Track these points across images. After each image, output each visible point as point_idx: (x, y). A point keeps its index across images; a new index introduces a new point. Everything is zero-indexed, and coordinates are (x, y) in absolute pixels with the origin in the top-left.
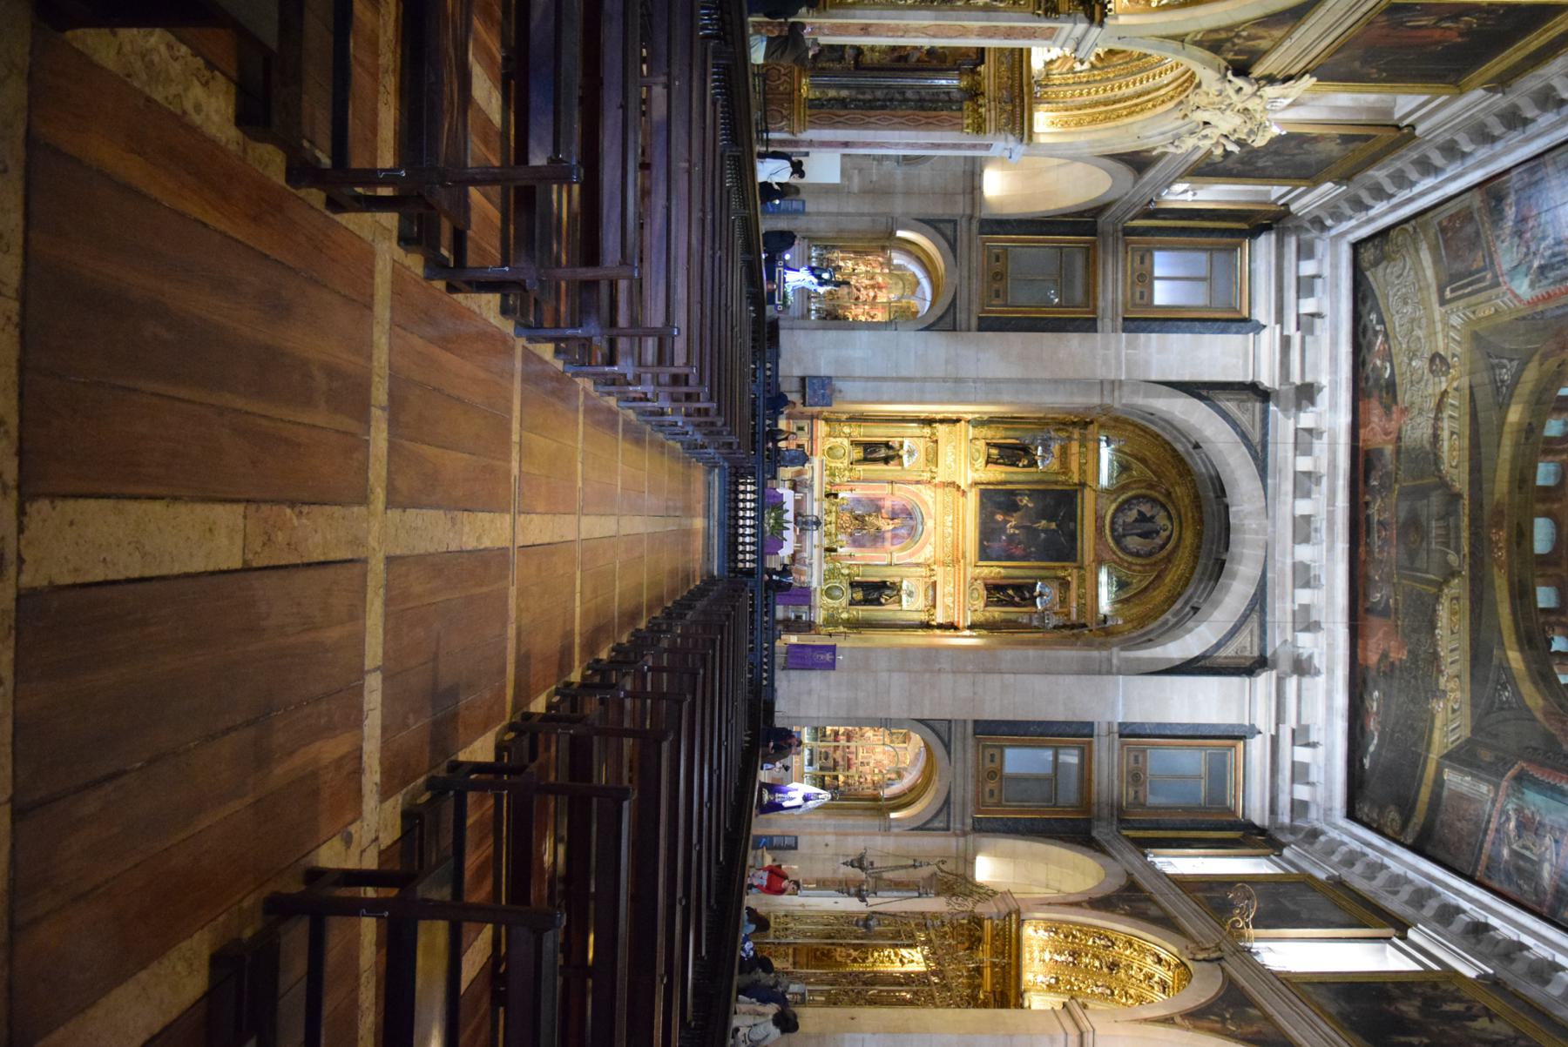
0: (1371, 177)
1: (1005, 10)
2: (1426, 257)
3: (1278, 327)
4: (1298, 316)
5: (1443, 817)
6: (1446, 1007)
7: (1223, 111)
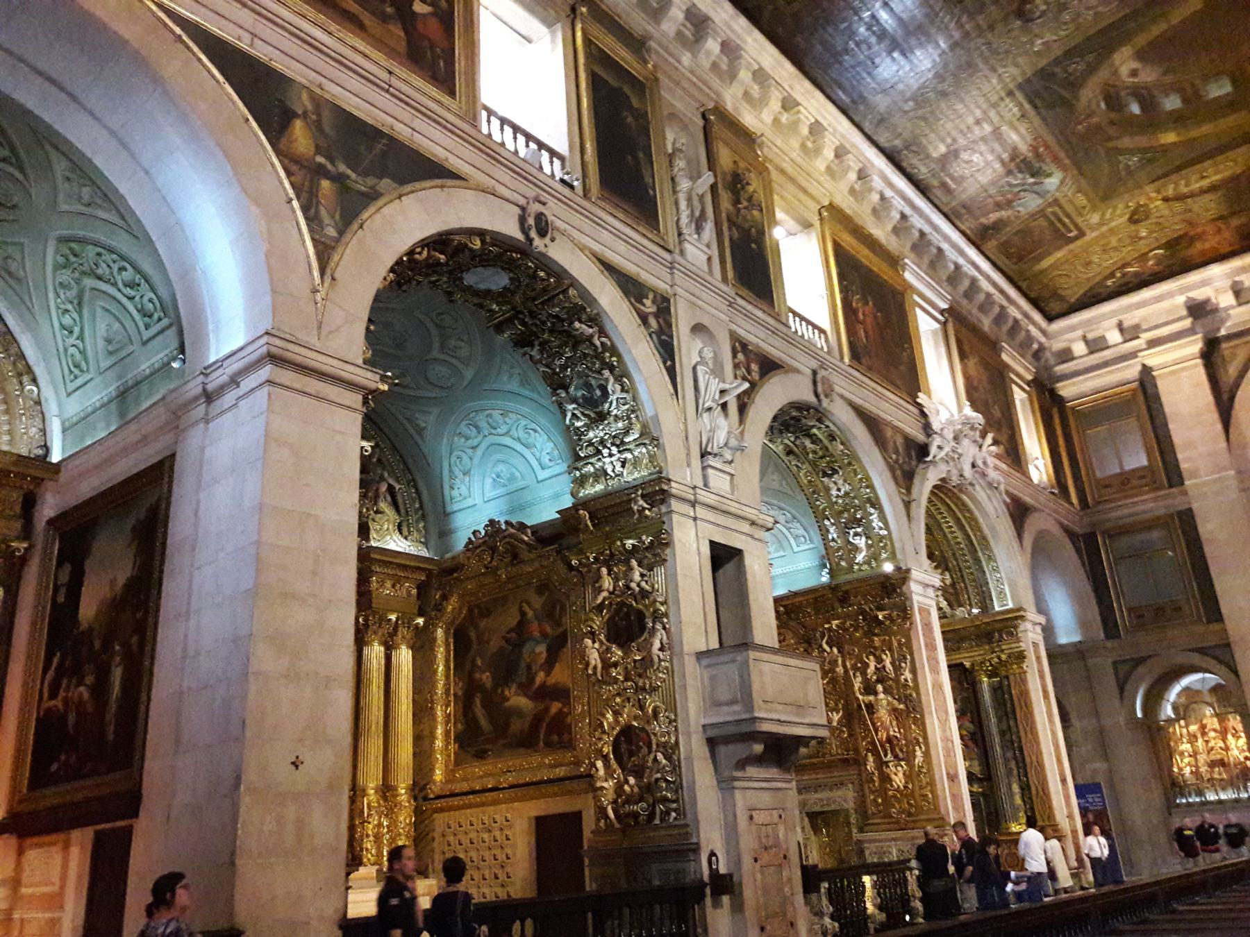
0: (991, 328)
1: (912, 654)
2: (1045, 264)
3: (1140, 354)
4: (1125, 341)
7: (961, 455)
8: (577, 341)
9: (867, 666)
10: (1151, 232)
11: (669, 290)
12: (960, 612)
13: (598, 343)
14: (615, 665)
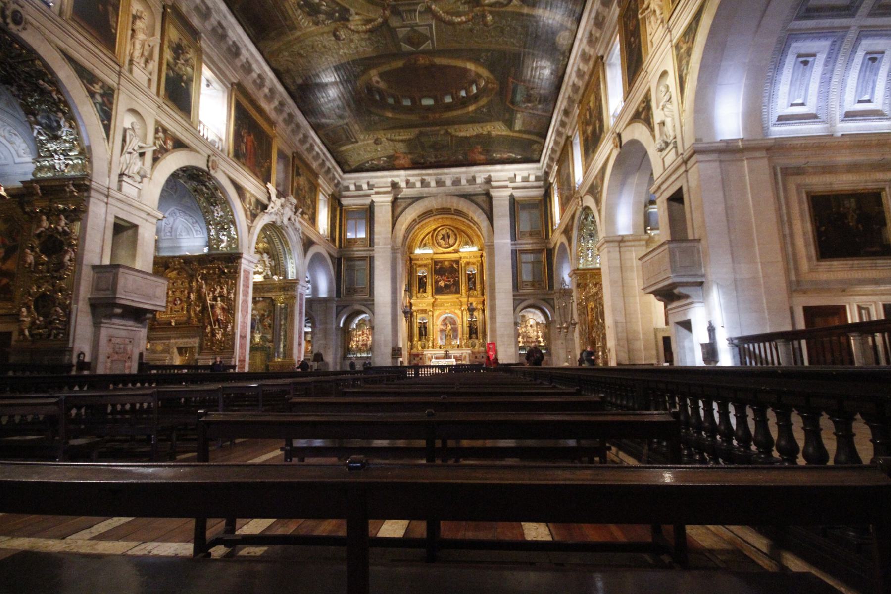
2: (344, 148)
5: (532, 129)
6: (588, 117)
7: (282, 214)
8: (42, 92)
9: (215, 290)
10: (382, 150)
11: (116, 85)
12: (275, 278)
13: (55, 97)
14: (42, 264)
